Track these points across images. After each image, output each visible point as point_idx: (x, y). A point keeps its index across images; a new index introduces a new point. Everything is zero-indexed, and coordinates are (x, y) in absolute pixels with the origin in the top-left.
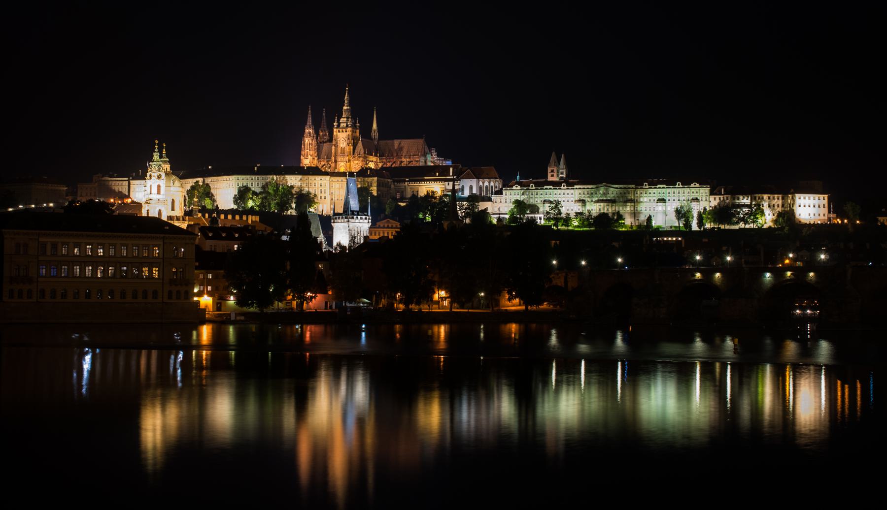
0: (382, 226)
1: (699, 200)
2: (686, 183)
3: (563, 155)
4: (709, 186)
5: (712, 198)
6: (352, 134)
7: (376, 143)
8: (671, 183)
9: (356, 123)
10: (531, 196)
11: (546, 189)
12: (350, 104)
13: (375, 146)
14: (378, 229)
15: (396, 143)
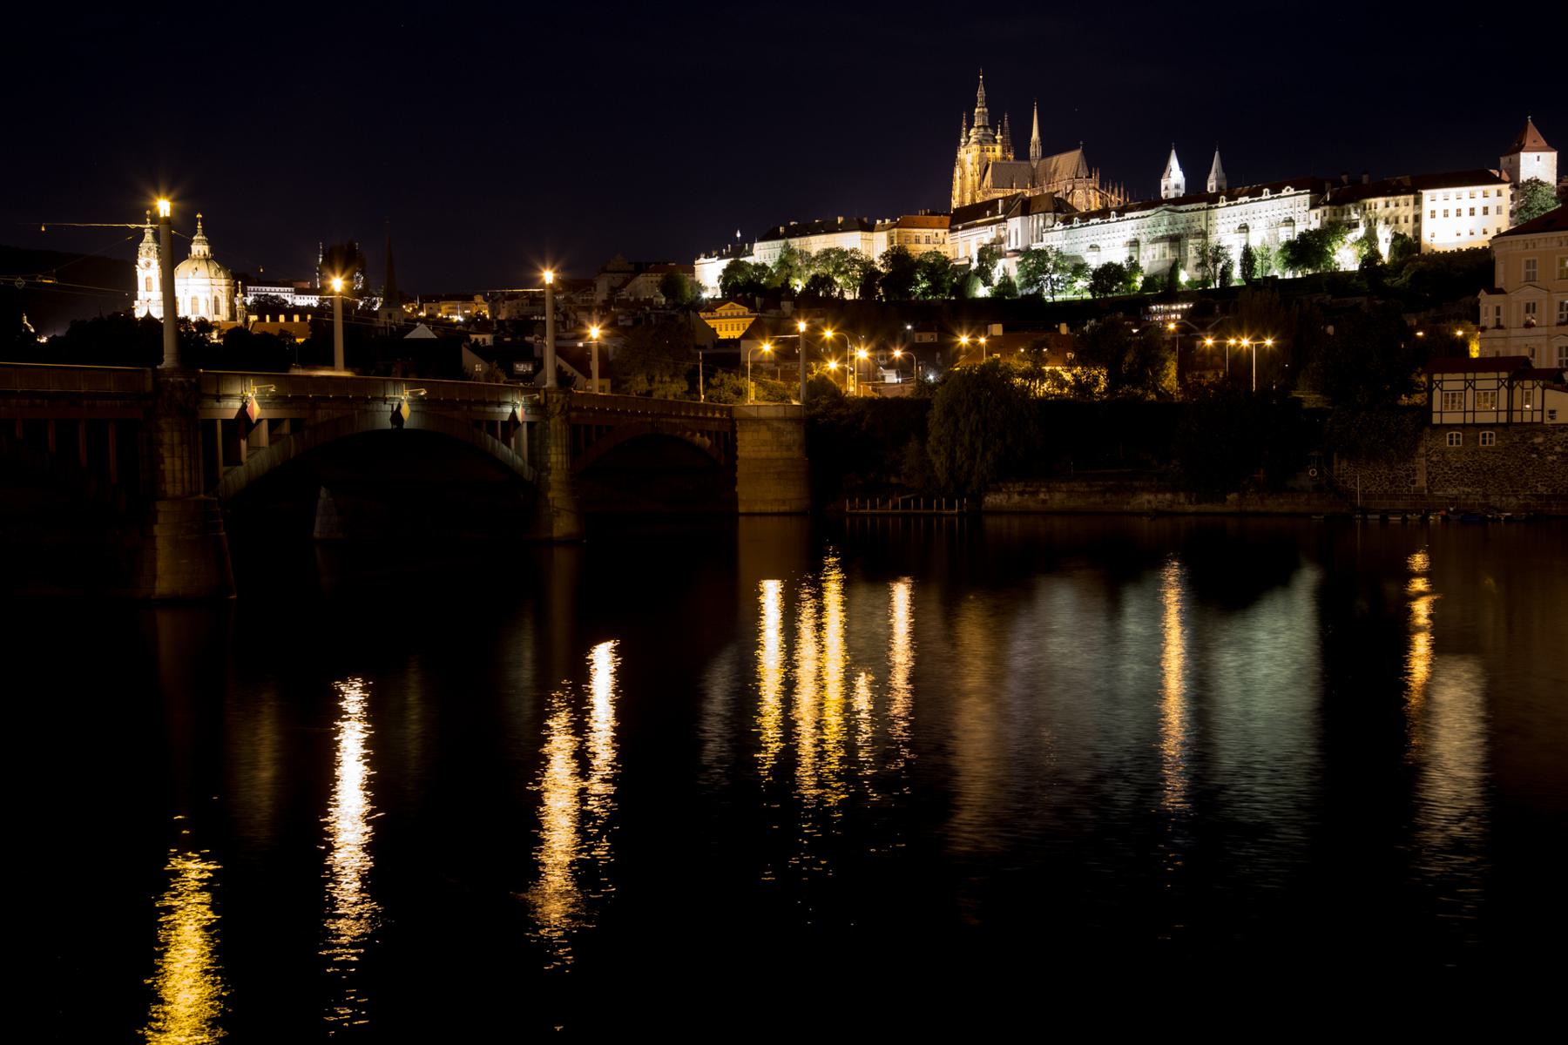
0: (723, 315)
1: (1293, 221)
2: (1276, 190)
3: (1217, 153)
4: (1308, 191)
5: (1313, 212)
6: (980, 156)
7: (1036, 164)
8: (1255, 193)
9: (996, 134)
10: (1076, 240)
11: (1093, 224)
12: (988, 103)
13: (1034, 169)
14: (718, 320)
15: (1055, 158)
